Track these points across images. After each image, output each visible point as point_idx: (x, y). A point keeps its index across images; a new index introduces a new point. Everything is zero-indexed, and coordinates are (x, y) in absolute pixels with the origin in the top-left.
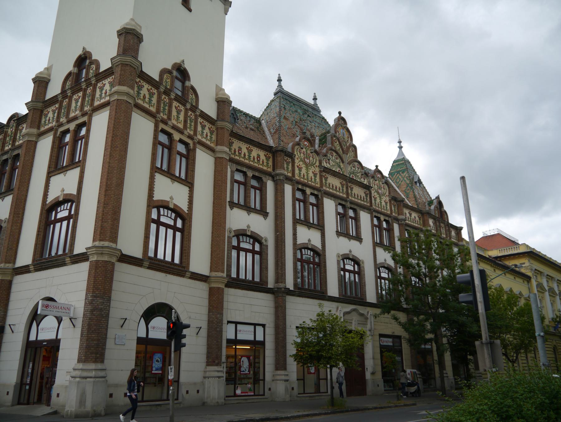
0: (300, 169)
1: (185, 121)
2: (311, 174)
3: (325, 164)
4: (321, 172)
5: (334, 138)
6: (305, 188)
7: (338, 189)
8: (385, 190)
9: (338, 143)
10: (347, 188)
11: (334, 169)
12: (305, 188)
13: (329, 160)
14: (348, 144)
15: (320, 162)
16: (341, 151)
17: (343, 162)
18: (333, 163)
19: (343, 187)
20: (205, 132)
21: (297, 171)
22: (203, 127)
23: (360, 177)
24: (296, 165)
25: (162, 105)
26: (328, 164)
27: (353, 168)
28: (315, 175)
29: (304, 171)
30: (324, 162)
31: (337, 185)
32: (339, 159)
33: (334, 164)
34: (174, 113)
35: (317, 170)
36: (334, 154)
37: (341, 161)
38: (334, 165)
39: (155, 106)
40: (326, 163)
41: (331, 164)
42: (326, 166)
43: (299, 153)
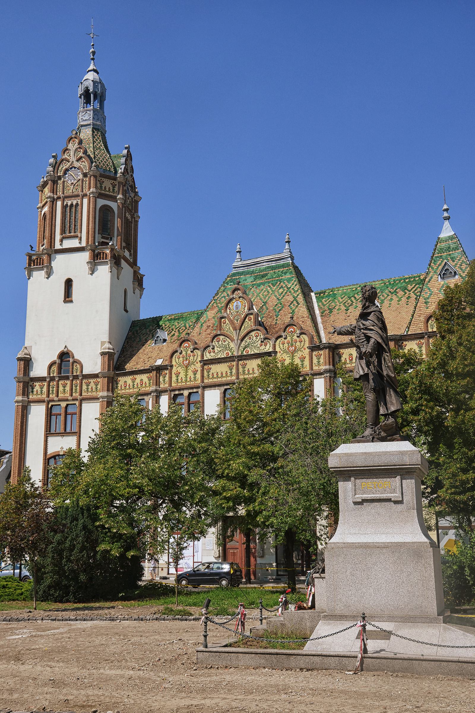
0: (177, 375)
1: (71, 389)
2: (190, 374)
3: (208, 356)
4: (203, 367)
5: (223, 320)
6: (182, 392)
7: (224, 375)
8: (303, 343)
9: (227, 322)
10: (238, 369)
11: (219, 356)
12: (182, 392)
13: (213, 349)
14: (242, 316)
15: (202, 356)
16: (231, 328)
17: (232, 340)
18: (219, 349)
19: (231, 370)
20: (90, 387)
21: (174, 378)
22: (88, 385)
23: (259, 346)
24: (173, 373)
25: (51, 389)
26: (212, 354)
27: (248, 341)
28: (195, 372)
29: (182, 375)
30: (207, 353)
31: (222, 371)
32: (228, 339)
33: (219, 349)
34: (61, 388)
35: (198, 366)
36: (221, 337)
37: (230, 341)
38: (221, 351)
39: (45, 393)
40: (210, 353)
41: (216, 351)
42: (210, 358)
43: (177, 360)
